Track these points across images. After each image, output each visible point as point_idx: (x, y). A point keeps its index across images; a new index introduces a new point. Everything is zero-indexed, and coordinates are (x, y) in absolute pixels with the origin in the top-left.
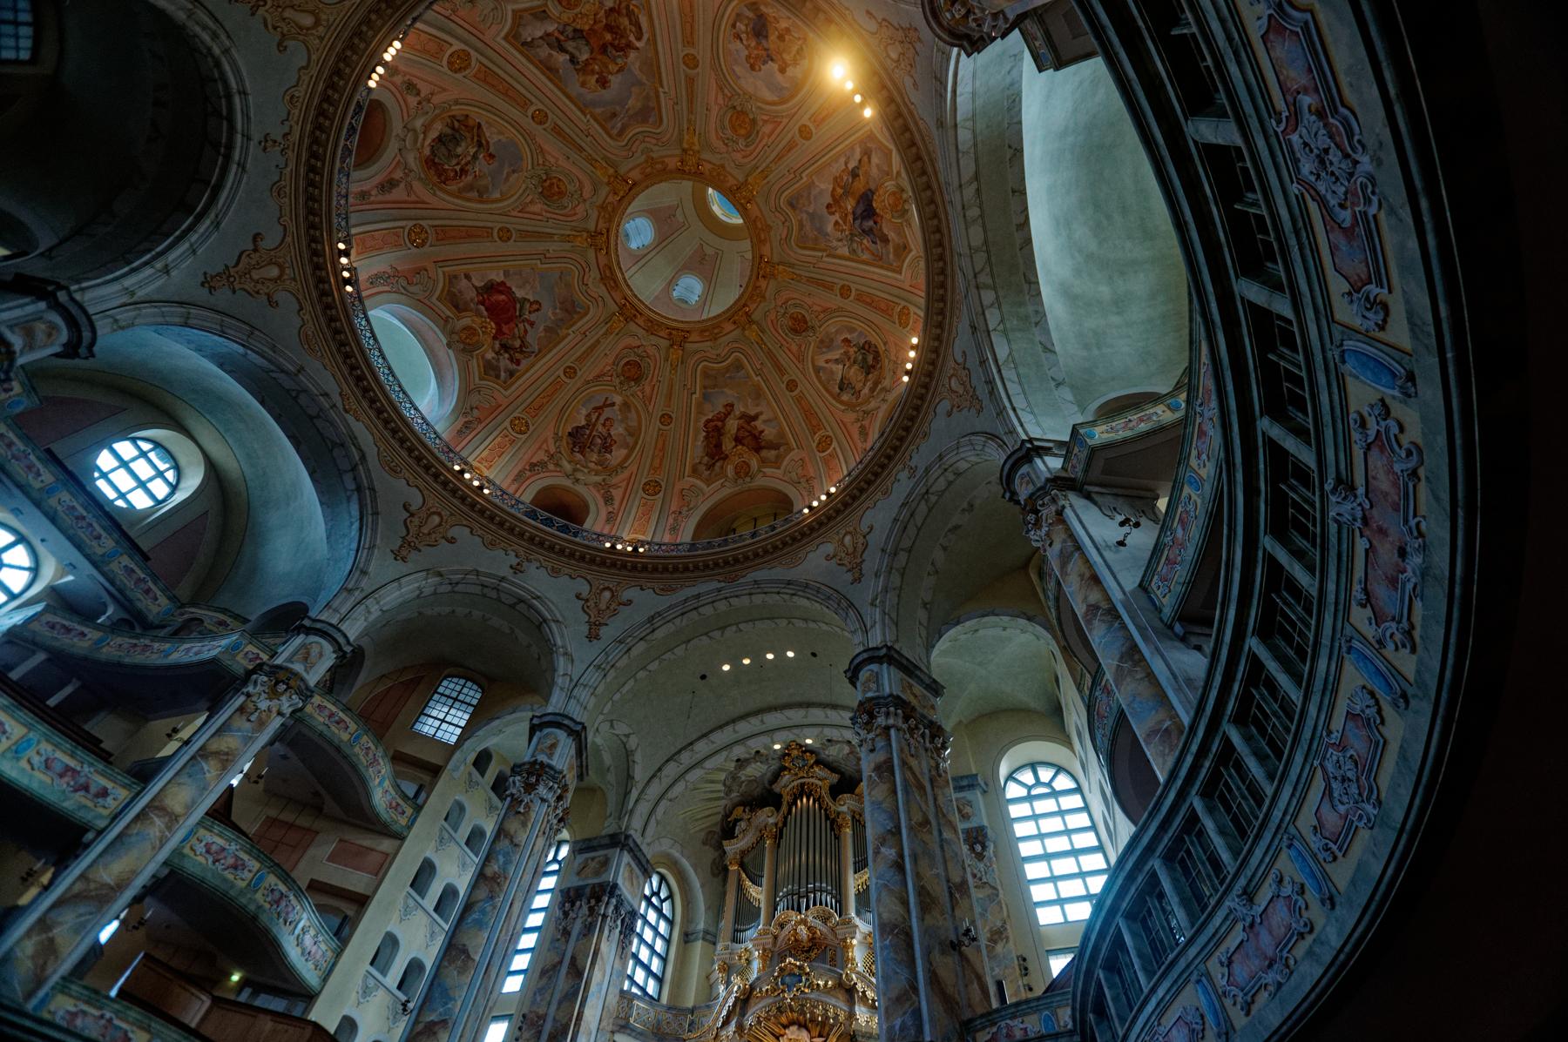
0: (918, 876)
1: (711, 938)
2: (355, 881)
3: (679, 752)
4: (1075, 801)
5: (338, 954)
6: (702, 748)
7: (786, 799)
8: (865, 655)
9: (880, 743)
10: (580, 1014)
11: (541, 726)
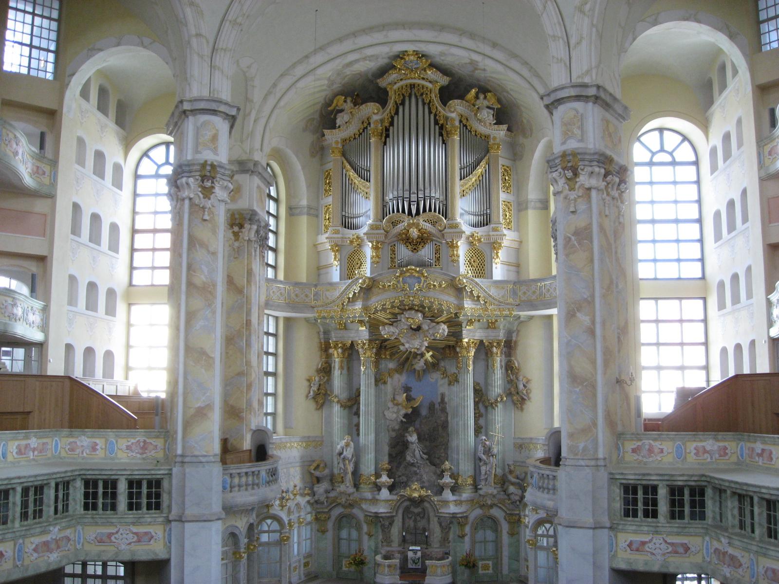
0: (604, 338)
1: (313, 212)
2: (31, 245)
3: (293, 66)
4: (689, 173)
5: (46, 310)
6: (319, 58)
7: (392, 99)
8: (573, 92)
9: (582, 206)
10: (248, 323)
11: (194, 112)
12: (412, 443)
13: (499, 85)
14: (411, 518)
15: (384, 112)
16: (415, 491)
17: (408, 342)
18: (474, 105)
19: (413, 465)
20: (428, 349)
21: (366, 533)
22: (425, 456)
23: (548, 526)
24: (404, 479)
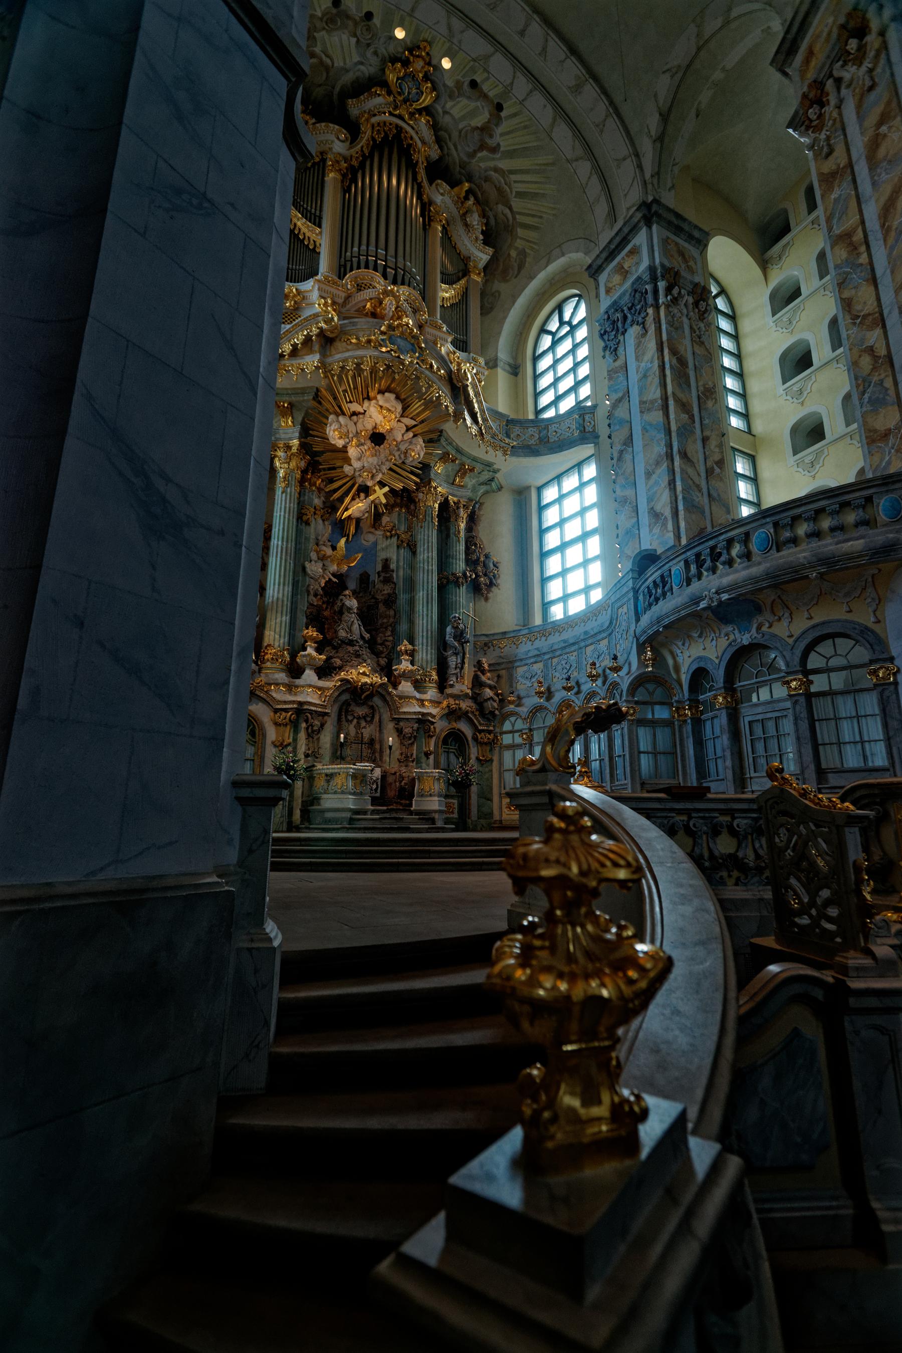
12: (349, 609)
13: (499, 190)
14: (351, 721)
15: (350, 148)
16: (363, 674)
17: (359, 459)
18: (462, 203)
19: (351, 643)
20: (382, 484)
21: (273, 743)
22: (367, 636)
23: (651, 687)
24: (338, 662)
